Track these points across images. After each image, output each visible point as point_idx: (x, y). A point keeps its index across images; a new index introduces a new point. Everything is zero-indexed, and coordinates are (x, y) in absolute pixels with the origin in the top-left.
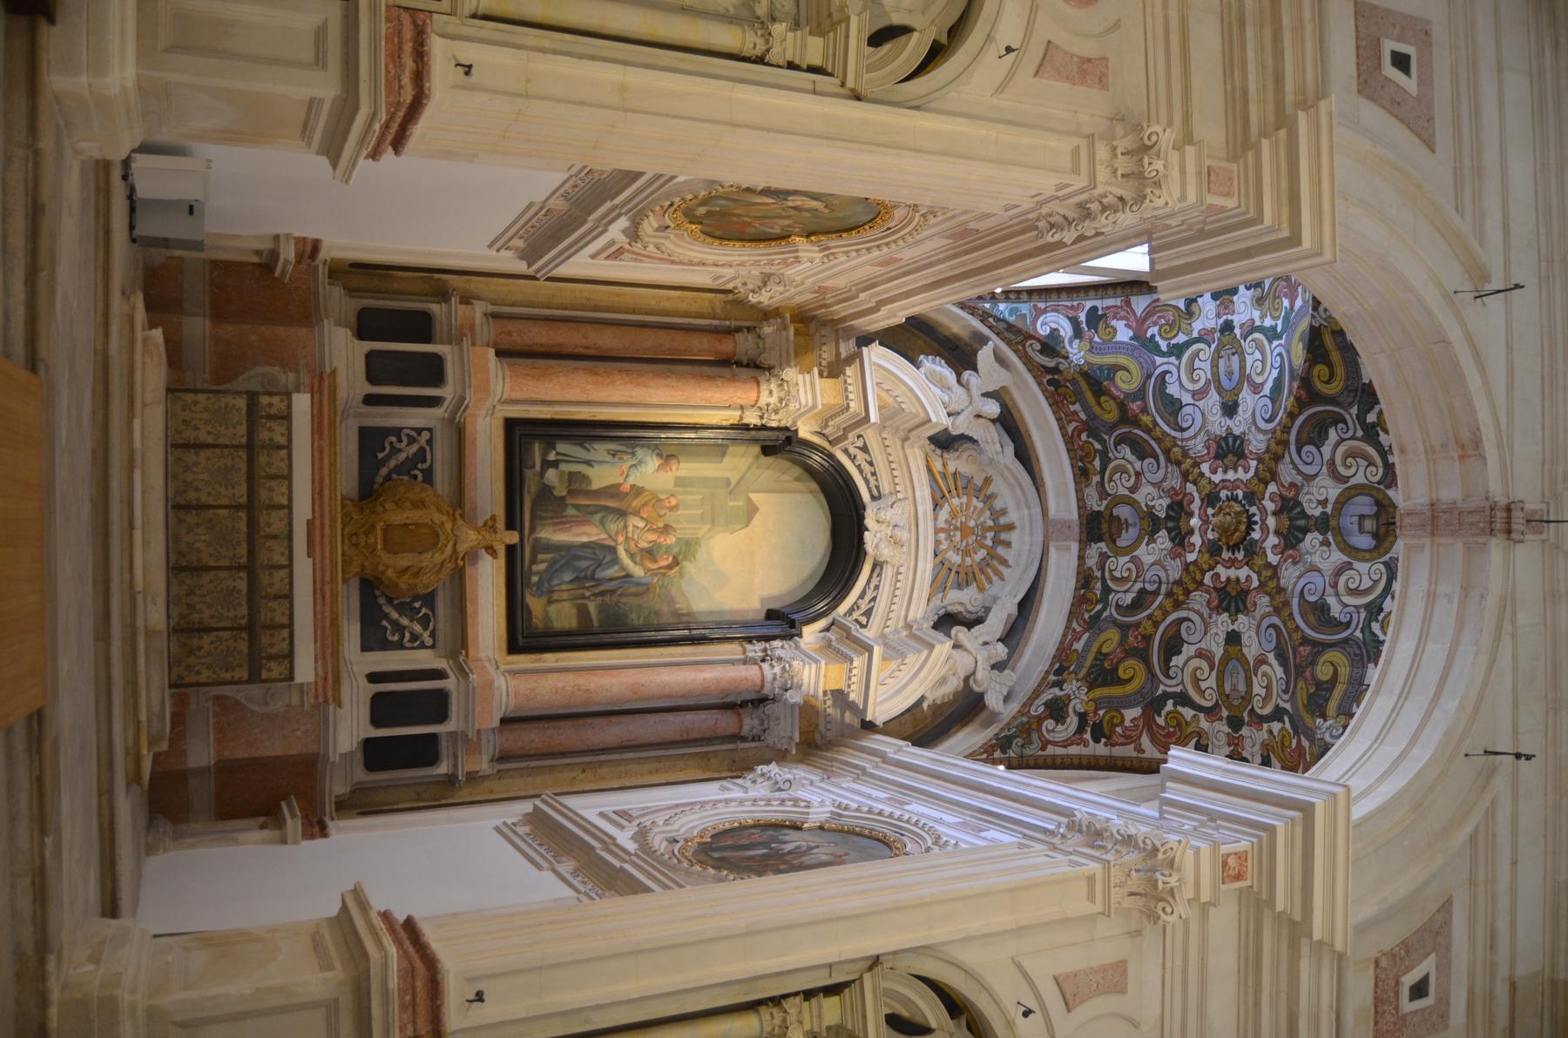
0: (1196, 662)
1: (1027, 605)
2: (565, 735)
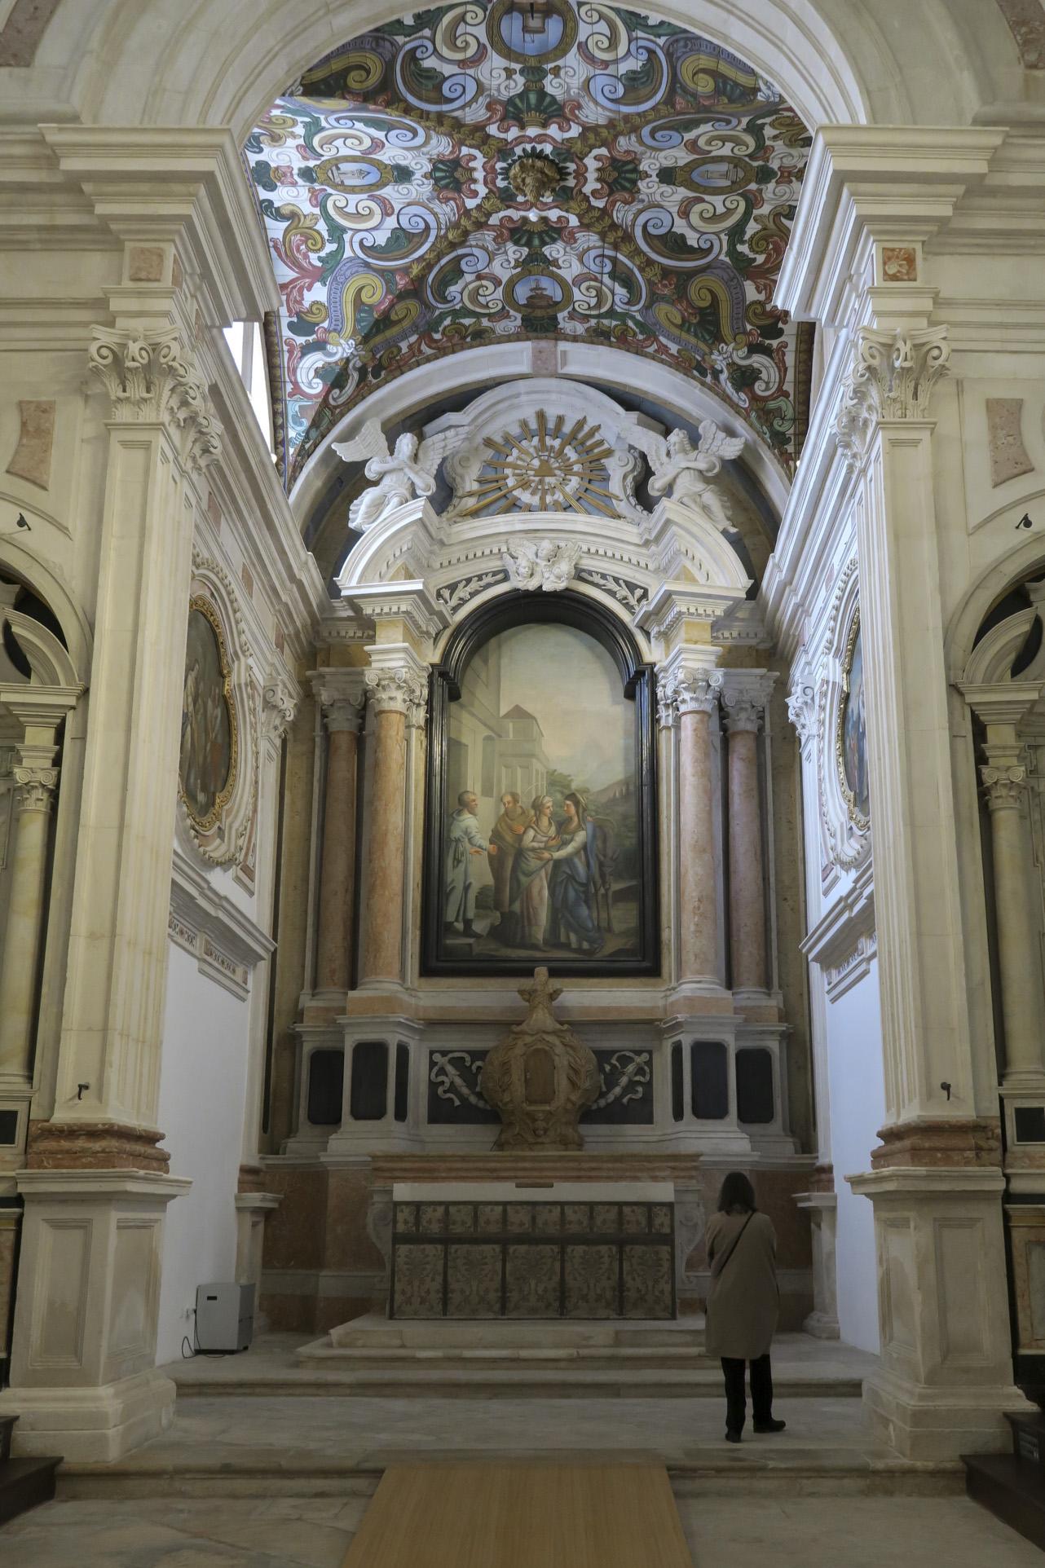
0: (694, 218)
1: (628, 400)
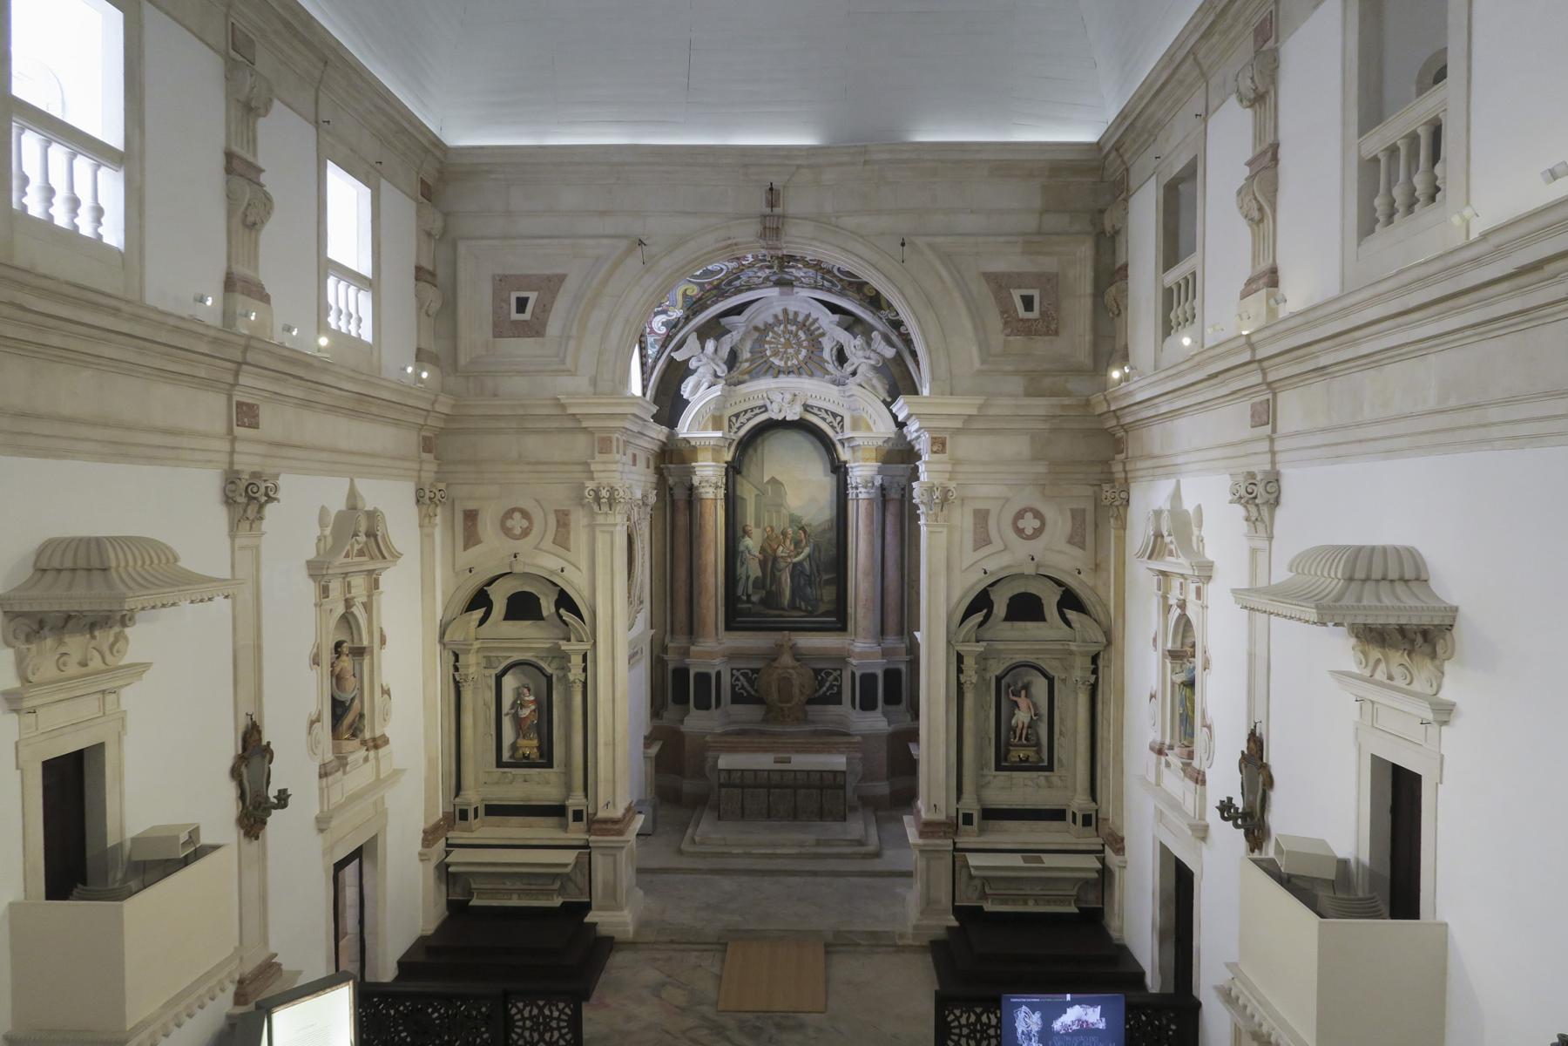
1: (834, 309)
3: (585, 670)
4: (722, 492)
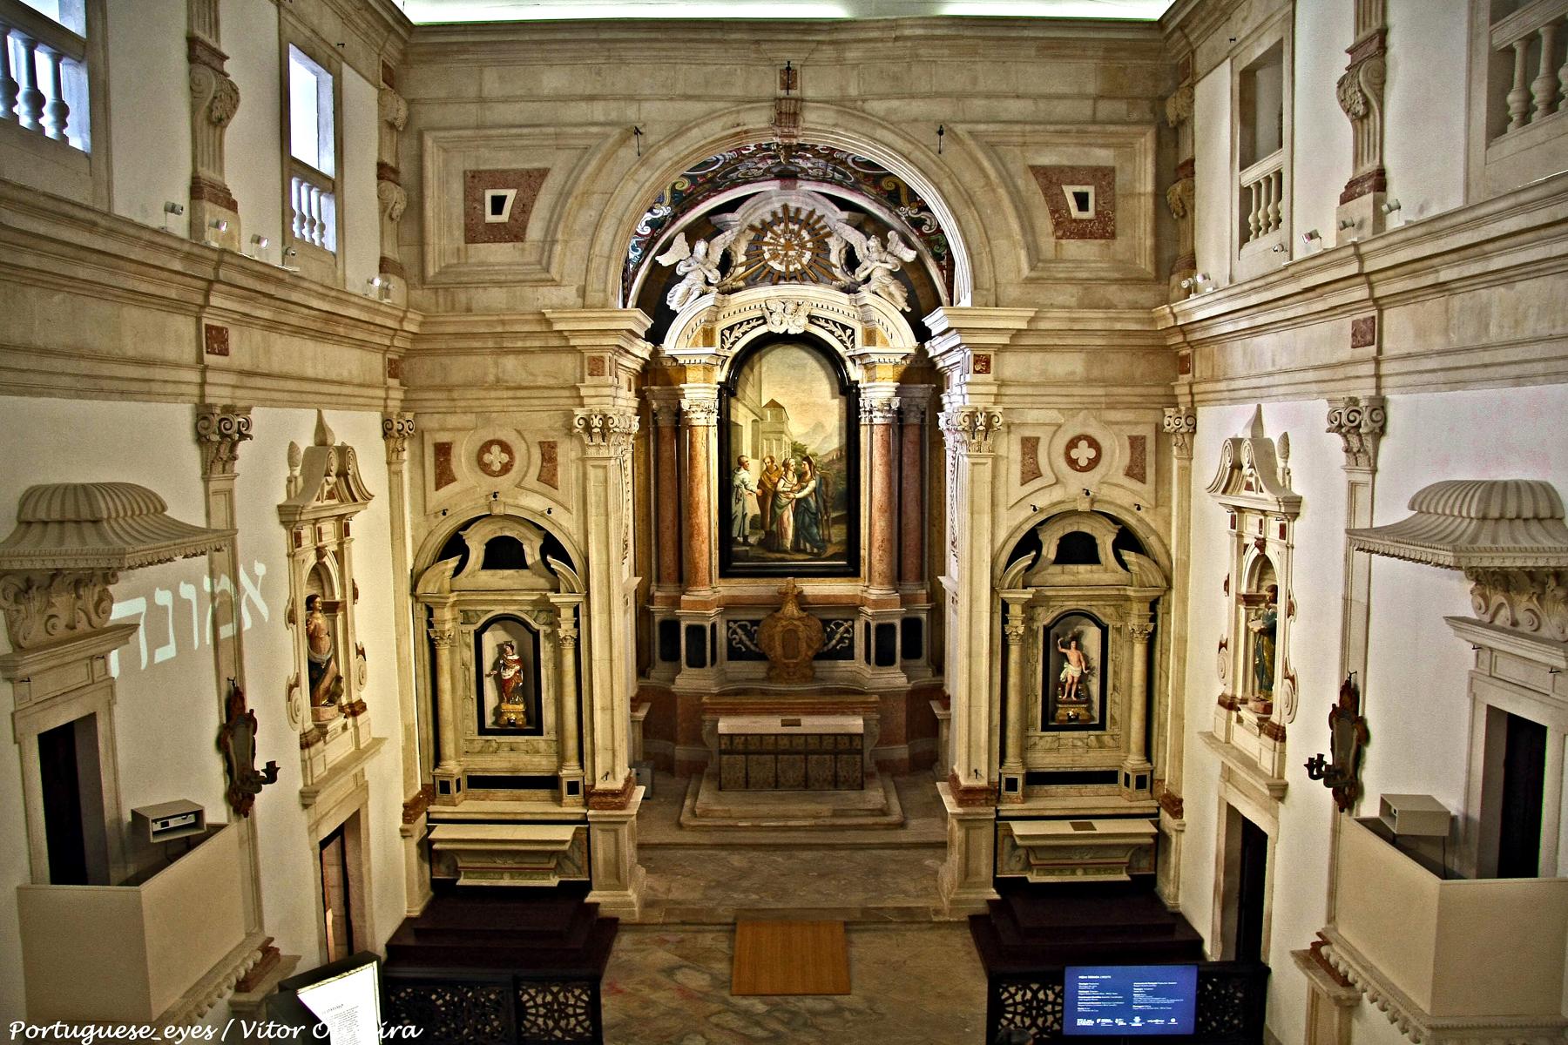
1: (843, 205)
2: (911, 540)
3: (577, 625)
4: (714, 418)
